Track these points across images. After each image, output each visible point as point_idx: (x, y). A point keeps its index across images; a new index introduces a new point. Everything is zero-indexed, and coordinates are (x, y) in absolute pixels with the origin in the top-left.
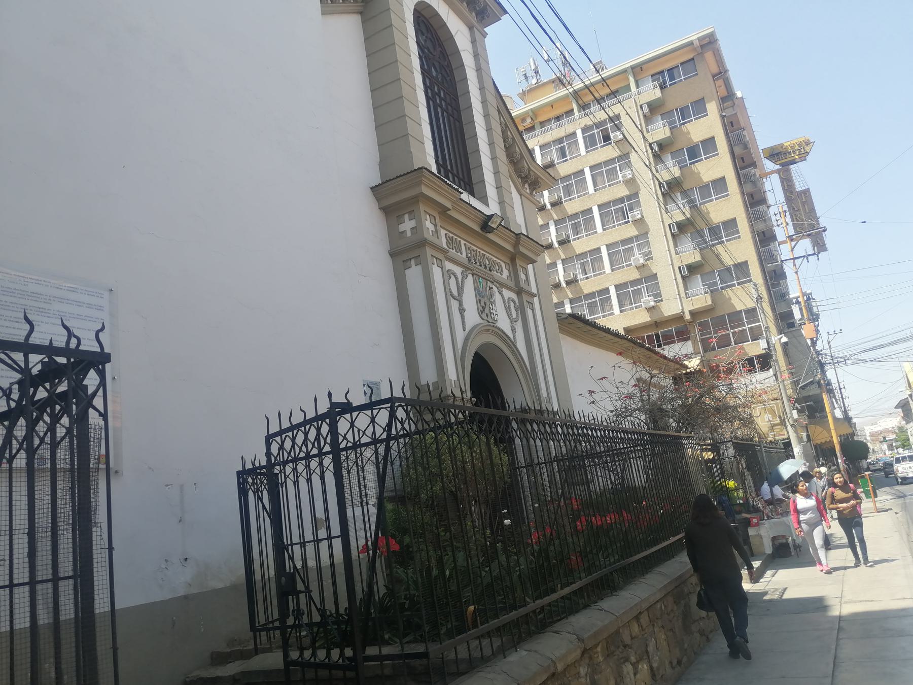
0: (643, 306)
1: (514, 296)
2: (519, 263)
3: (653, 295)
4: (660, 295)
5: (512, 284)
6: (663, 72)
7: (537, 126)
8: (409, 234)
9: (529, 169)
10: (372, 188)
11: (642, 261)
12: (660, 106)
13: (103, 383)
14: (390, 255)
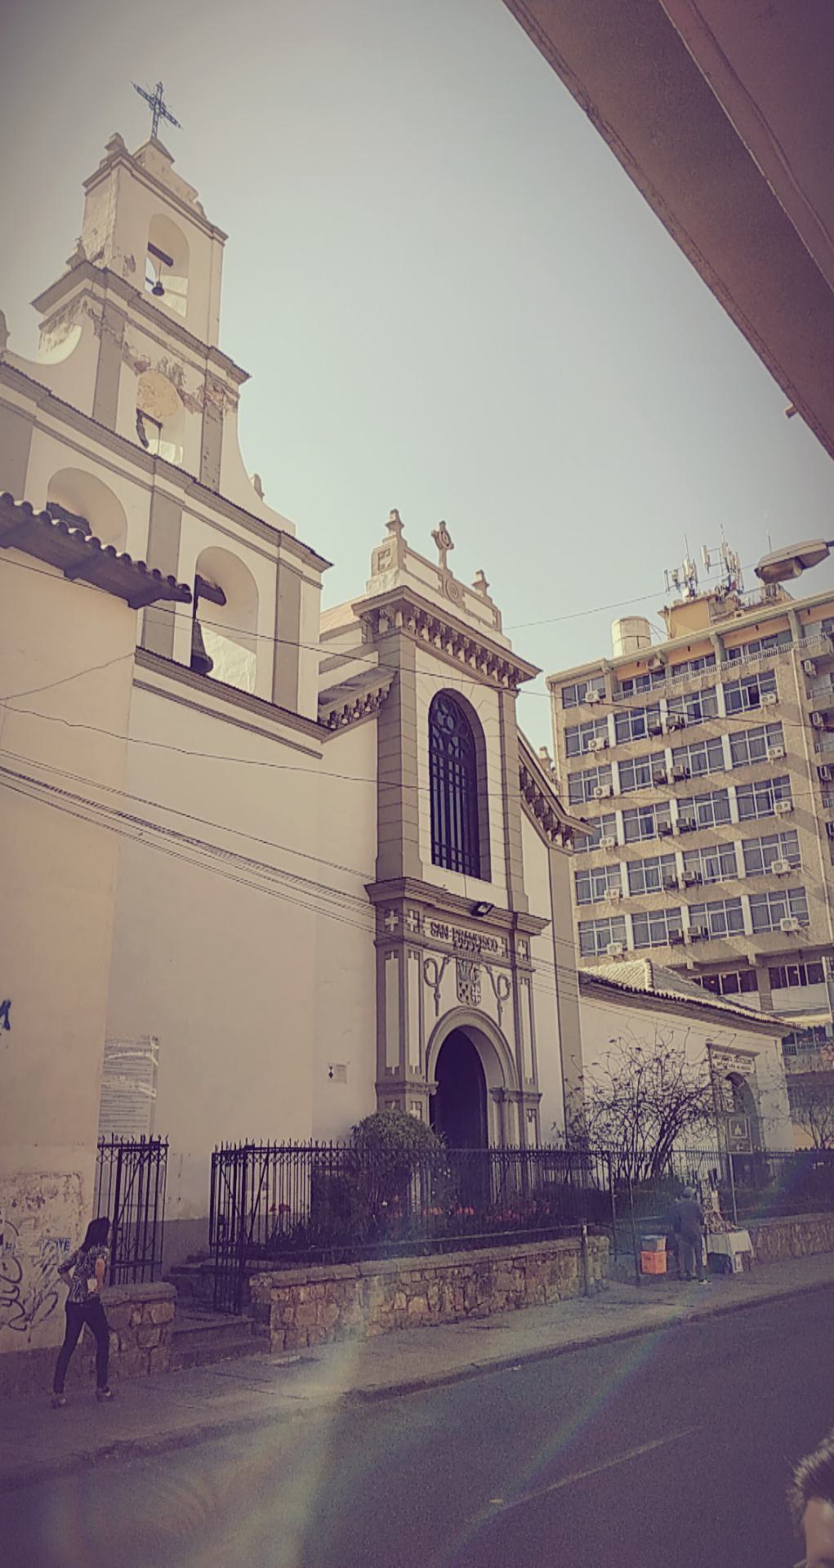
1: (508, 972)
2: (517, 936)
3: (797, 916)
4: (806, 916)
5: (508, 960)
8: (392, 929)
9: (559, 823)
10: (366, 886)
11: (786, 868)
13: (166, 1153)
14: (376, 946)
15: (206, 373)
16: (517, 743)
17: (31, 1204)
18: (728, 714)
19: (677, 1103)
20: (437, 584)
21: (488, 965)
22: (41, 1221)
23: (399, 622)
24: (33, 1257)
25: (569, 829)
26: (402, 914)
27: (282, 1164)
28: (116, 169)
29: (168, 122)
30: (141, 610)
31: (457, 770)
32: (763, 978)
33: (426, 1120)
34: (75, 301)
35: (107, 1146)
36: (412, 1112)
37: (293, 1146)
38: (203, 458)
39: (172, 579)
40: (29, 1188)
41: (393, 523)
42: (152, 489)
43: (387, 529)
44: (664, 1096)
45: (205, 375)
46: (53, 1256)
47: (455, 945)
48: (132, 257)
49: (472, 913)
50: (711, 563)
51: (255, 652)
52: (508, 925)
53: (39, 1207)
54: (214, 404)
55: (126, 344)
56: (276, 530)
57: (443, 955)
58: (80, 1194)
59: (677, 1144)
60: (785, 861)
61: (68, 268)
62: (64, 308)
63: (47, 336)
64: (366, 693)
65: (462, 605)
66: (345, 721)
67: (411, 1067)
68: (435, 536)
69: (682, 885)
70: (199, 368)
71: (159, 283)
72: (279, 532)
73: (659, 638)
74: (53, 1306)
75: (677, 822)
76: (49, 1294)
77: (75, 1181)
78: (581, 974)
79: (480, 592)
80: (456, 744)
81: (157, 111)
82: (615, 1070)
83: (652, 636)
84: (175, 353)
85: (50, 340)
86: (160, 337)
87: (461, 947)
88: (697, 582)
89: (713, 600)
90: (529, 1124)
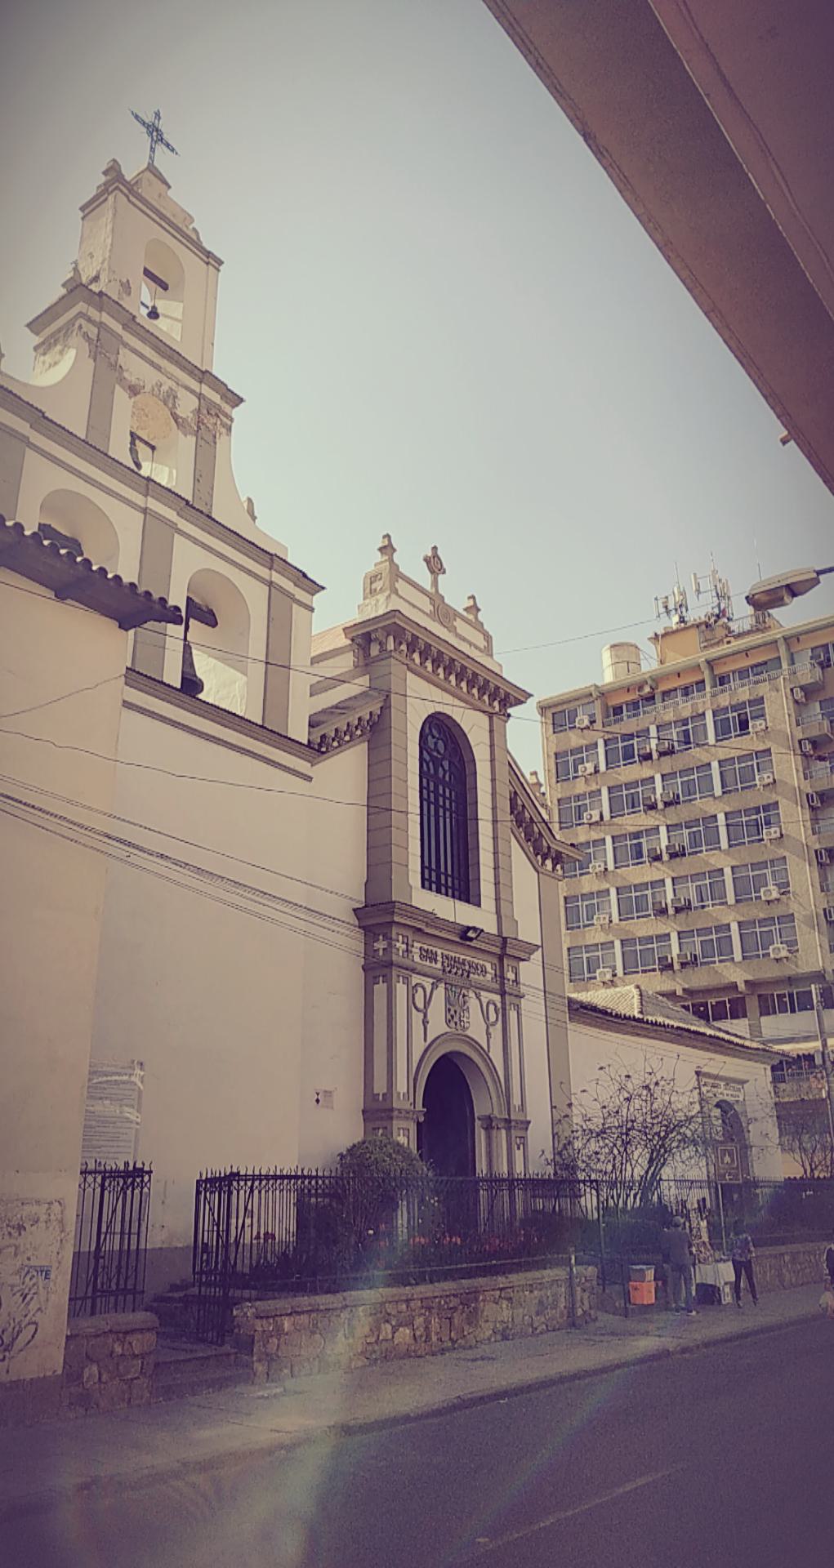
0: (772, 956)
1: (497, 998)
3: (786, 942)
5: (497, 986)
6: (827, 645)
7: (658, 698)
8: (381, 953)
9: (549, 848)
10: (354, 910)
11: (775, 895)
12: (819, 690)
13: (150, 1180)
15: (200, 396)
16: (508, 767)
17: (12, 1231)
18: (717, 741)
19: (666, 1131)
20: (428, 608)
21: (477, 991)
22: (22, 1249)
23: (391, 645)
24: (12, 1286)
25: (559, 853)
26: (391, 939)
27: (267, 1192)
28: (114, 194)
29: (165, 149)
30: (132, 632)
31: (448, 794)
32: (752, 1004)
33: (413, 1147)
34: (72, 322)
35: (90, 1173)
36: (399, 1139)
37: (278, 1173)
38: (196, 480)
39: (163, 600)
40: (10, 1215)
41: (385, 547)
42: (145, 511)
43: (379, 553)
44: (653, 1124)
45: (199, 399)
46: (34, 1285)
47: (444, 970)
48: (128, 281)
49: (461, 938)
50: (701, 590)
51: (246, 675)
52: (497, 951)
53: (20, 1234)
54: (207, 427)
55: (121, 367)
56: (268, 553)
57: (431, 980)
58: (61, 1222)
59: (666, 1172)
60: (775, 887)
61: (63, 291)
62: (59, 330)
63: (42, 358)
64: (357, 716)
65: (453, 630)
66: (335, 744)
67: (399, 1093)
68: (427, 560)
69: (671, 911)
70: (193, 392)
71: (154, 307)
72: (271, 555)
73: (650, 664)
74: (33, 1337)
75: (667, 847)
76: (29, 1324)
77: (56, 1208)
78: (570, 1001)
79: (471, 617)
80: (447, 768)
81: (155, 138)
82: (604, 1097)
83: (642, 663)
84: (170, 377)
85: (44, 363)
86: (155, 360)
87: (450, 972)
88: (687, 610)
89: (704, 627)
90: (517, 1151)
